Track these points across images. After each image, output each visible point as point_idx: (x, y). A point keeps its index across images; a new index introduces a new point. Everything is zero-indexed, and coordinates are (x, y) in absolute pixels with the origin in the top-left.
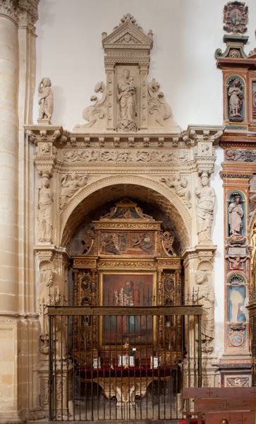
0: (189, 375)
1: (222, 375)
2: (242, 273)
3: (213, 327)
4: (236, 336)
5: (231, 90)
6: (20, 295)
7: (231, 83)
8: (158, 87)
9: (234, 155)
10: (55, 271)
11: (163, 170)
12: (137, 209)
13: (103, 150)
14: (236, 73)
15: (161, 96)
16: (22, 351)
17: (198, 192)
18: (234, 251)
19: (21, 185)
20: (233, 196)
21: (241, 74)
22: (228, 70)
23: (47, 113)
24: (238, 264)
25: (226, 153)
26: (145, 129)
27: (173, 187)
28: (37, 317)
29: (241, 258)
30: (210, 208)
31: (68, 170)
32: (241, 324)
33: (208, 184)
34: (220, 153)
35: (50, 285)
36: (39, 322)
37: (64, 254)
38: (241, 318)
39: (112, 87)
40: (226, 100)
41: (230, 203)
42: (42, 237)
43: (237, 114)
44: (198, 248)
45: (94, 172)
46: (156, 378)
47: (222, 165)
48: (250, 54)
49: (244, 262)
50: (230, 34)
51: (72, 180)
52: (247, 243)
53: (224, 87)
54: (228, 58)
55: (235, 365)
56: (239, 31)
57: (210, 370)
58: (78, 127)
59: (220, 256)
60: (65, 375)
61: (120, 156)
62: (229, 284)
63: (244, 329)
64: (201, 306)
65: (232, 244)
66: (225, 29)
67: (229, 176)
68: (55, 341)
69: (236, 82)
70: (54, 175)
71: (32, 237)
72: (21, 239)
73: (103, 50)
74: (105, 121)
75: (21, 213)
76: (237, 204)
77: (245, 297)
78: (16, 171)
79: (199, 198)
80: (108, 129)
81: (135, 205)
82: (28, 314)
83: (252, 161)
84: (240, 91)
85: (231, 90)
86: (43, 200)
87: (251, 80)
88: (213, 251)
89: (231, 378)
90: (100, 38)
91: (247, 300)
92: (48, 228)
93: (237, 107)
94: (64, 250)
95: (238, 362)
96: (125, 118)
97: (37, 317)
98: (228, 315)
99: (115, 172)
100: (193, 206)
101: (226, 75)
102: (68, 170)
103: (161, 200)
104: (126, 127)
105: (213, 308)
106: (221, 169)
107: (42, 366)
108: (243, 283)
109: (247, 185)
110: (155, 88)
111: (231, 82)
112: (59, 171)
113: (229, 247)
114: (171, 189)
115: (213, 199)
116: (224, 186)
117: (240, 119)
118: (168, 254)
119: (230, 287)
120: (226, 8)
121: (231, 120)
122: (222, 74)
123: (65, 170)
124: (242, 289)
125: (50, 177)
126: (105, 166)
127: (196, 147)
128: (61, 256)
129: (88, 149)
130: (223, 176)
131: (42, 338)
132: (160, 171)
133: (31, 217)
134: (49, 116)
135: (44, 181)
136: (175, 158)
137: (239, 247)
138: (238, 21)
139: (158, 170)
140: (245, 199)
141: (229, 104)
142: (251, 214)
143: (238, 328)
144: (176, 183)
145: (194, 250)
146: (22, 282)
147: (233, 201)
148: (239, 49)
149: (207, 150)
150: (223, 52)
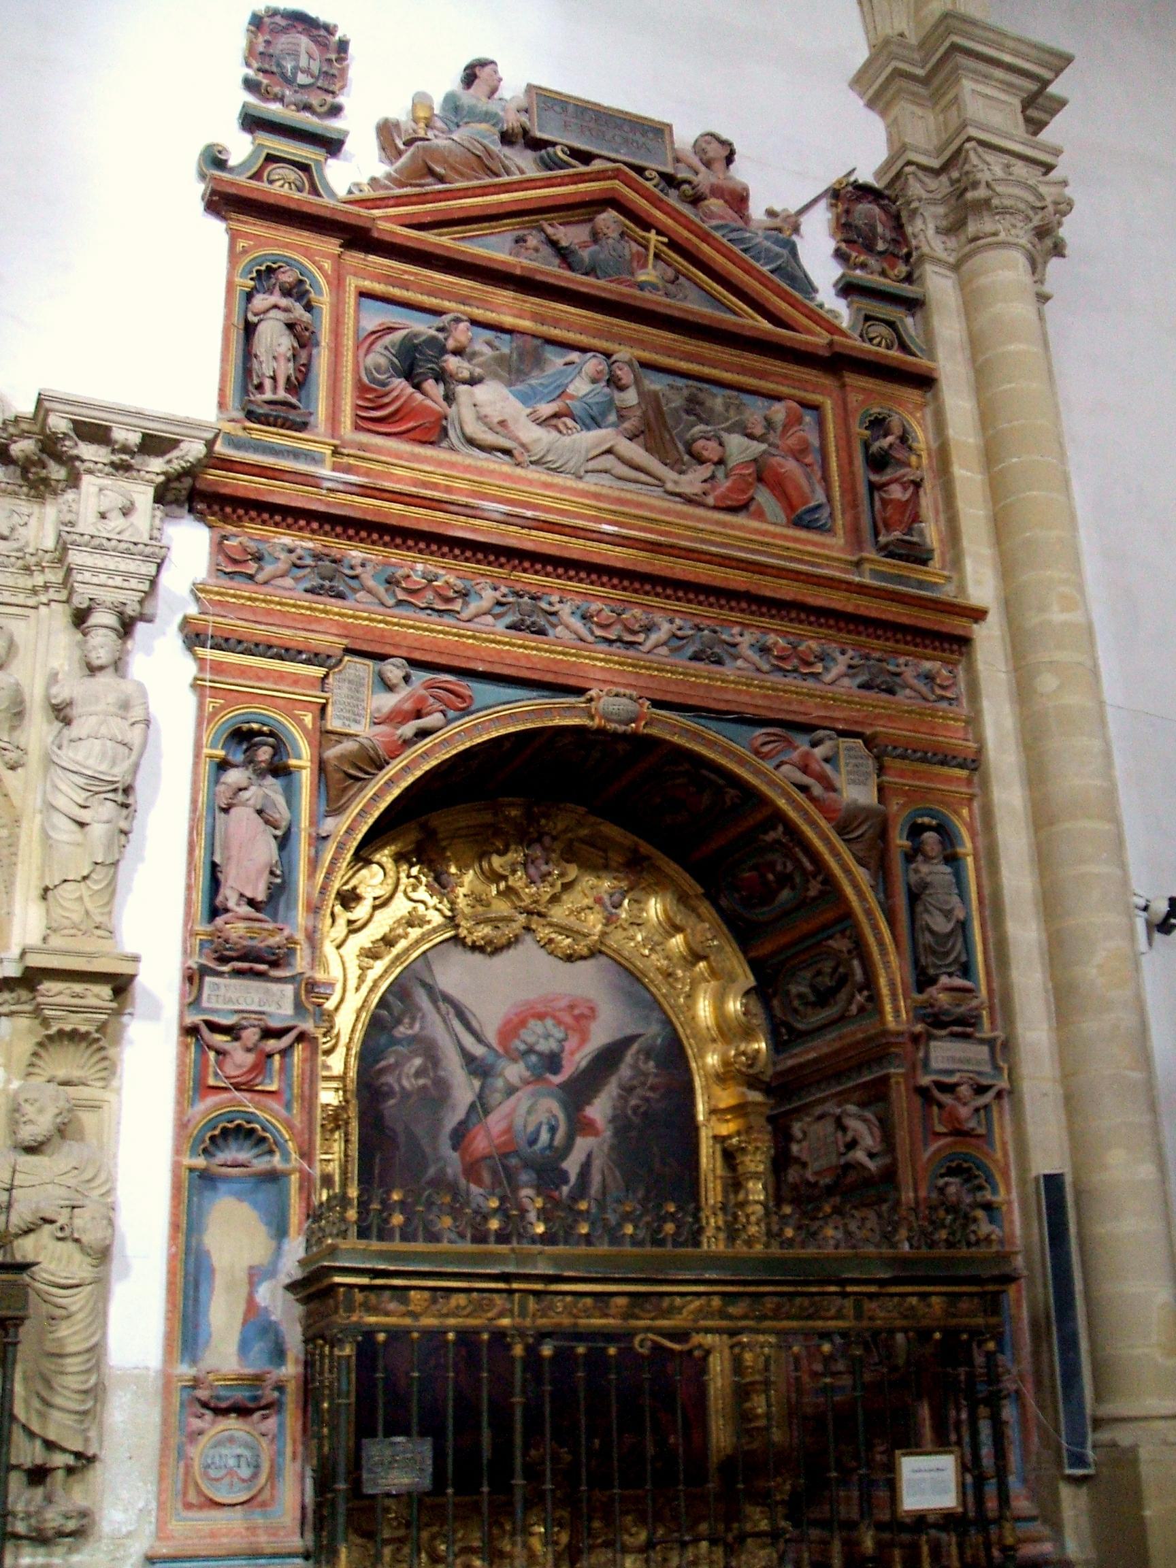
2: (267, 1114)
3: (96, 1393)
5: (260, 301)
9: (258, 558)
14: (287, 246)
17: (61, 693)
20: (242, 736)
24: (250, 1059)
25: (219, 546)
29: (269, 1033)
30: (119, 773)
32: (258, 1379)
33: (118, 665)
38: (259, 1347)
40: (237, 336)
41: (223, 765)
43: (282, 394)
44: (35, 961)
47: (198, 591)
48: (350, 192)
49: (285, 1053)
50: (274, 110)
52: (301, 963)
54: (254, 183)
56: (307, 107)
59: (155, 1013)
62: (200, 1162)
63: (274, 1406)
64: (24, 1267)
65: (223, 960)
66: (250, 85)
67: (224, 643)
69: (287, 277)
77: (280, 1231)
79: (67, 722)
83: (341, 596)
84: (299, 311)
87: (353, 284)
88: (121, 985)
91: (295, 1248)
93: (285, 369)
100: (34, 759)
101: (242, 243)
105: (101, 1285)
108: (276, 1161)
111: (265, 275)
113: (204, 971)
115: (135, 736)
117: (293, 415)
119: (205, 1180)
121: (251, 415)
122: (225, 239)
124: (267, 1193)
127: (70, 495)
130: (194, 637)
138: (307, 71)
140: (303, 759)
141: (248, 355)
142: (329, 825)
147: (239, 757)
148: (304, 168)
149: (126, 512)
150: (232, 162)
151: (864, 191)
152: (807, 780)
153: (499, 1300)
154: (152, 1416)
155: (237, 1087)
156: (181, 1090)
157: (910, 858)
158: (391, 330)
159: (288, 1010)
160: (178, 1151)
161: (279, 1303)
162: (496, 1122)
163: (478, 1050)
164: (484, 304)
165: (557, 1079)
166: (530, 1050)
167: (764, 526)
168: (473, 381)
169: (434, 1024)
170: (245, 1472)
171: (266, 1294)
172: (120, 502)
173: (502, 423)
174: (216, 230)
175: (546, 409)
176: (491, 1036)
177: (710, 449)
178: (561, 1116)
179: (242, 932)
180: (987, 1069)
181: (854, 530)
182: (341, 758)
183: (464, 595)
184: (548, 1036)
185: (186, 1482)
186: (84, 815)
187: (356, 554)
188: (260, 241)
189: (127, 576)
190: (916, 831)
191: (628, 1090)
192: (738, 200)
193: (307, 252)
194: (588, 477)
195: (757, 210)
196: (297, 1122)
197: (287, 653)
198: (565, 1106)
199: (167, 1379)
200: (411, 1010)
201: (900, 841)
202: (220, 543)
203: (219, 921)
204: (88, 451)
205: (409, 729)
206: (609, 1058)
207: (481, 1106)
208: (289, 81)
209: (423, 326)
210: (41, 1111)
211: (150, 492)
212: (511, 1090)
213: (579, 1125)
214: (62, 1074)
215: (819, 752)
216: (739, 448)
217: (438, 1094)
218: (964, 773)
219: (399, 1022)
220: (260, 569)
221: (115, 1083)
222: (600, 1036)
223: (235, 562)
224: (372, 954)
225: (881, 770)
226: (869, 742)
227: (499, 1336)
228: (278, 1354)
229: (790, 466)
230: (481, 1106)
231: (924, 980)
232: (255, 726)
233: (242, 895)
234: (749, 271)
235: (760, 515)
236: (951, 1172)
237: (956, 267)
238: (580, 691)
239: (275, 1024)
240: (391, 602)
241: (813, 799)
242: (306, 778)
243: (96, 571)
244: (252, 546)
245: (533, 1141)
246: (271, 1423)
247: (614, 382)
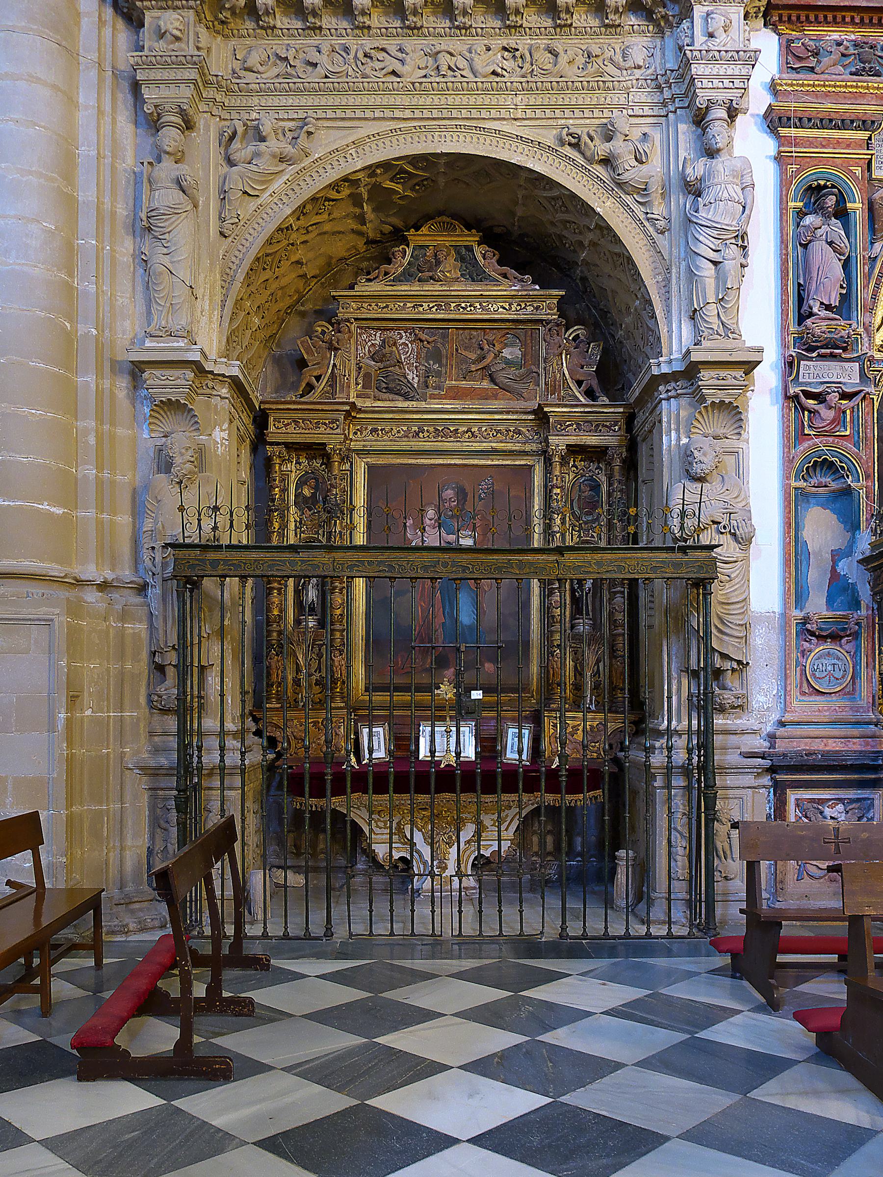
1: (779, 789)
12: (478, 251)
25: (787, 48)
29: (845, 396)
31: (249, 109)
37: (236, 385)
41: (801, 214)
45: (340, 114)
46: (550, 799)
55: (825, 754)
57: (739, 770)
62: (802, 484)
77: (853, 526)
81: (471, 239)
89: (812, 801)
99: (408, 114)
102: (249, 109)
103: (560, 216)
109: (863, 153)
118: (582, 399)
123: (238, 109)
126: (373, 91)
132: (563, 108)
137: (833, 357)
139: (553, 108)
145: (678, 367)
161: (855, 572)
171: (843, 567)
179: (824, 328)
185: (801, 679)
196: (863, 455)
197: (844, 124)
202: (788, 47)
203: (809, 322)
210: (705, 455)
220: (819, 62)
221: (744, 435)
223: (799, 59)
232: (822, 183)
233: (822, 303)
243: (710, 78)
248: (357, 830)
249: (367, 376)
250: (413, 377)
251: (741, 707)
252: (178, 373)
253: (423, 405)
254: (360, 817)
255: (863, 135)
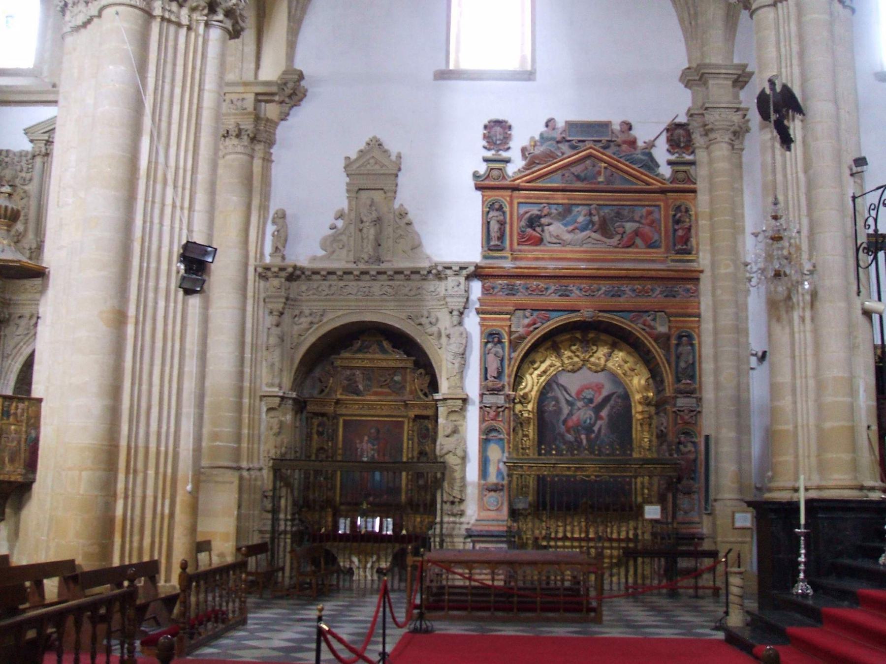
0: (435, 542)
2: (500, 426)
4: (492, 497)
5: (491, 214)
6: (242, 445)
7: (491, 207)
8: (406, 214)
9: (493, 288)
10: (283, 419)
11: (413, 306)
13: (342, 284)
15: (409, 224)
16: (242, 507)
17: (448, 332)
18: (490, 399)
19: (249, 325)
21: (504, 197)
22: (489, 193)
23: (280, 247)
24: (495, 413)
25: (483, 287)
26: (389, 261)
27: (420, 324)
28: (261, 469)
29: (498, 407)
34: (476, 287)
35: (278, 434)
36: (262, 476)
37: (294, 399)
38: (500, 477)
39: (353, 215)
41: (487, 343)
42: (270, 381)
49: (503, 411)
51: (306, 317)
53: (483, 211)
58: (314, 259)
59: (474, 403)
60: (289, 536)
61: (361, 289)
63: (502, 490)
68: (280, 497)
69: (497, 206)
70: (286, 311)
71: (258, 381)
72: (246, 384)
73: (345, 174)
74: (344, 252)
75: (248, 355)
76: (495, 345)
77: (503, 452)
78: (244, 310)
80: (347, 262)
82: (251, 466)
83: (514, 295)
85: (490, 216)
86: (273, 340)
87: (516, 201)
90: (342, 164)
92: (276, 369)
94: (294, 395)
95: (492, 528)
96: (365, 250)
97: (261, 469)
98: (484, 472)
100: (444, 347)
101: (485, 198)
104: (367, 262)
106: (478, 306)
107: (264, 525)
108: (501, 436)
110: (403, 214)
111: (491, 207)
112: (291, 307)
114: (419, 327)
116: (482, 326)
120: (486, 127)
121: (490, 250)
122: (481, 197)
125: (282, 314)
128: (290, 402)
129: (325, 282)
130: (478, 313)
131: (266, 494)
133: (259, 359)
134: (282, 249)
135: (274, 319)
136: (424, 292)
137: (497, 394)
138: (499, 140)
140: (506, 340)
142: (514, 355)
143: (495, 489)
144: (424, 321)
146: (245, 431)
151: (680, 126)
152: (644, 327)
153: (544, 468)
154: (476, 491)
155: (492, 420)
156: (480, 421)
157: (678, 345)
158: (527, 213)
159: (503, 402)
160: (480, 435)
162: (575, 418)
163: (570, 399)
164: (553, 198)
165: (592, 405)
166: (585, 398)
167: (554, 320)
168: (549, 225)
169: (558, 393)
170: (495, 503)
172: (457, 284)
173: (558, 236)
174: (479, 194)
175: (570, 228)
176: (573, 394)
177: (620, 230)
178: (593, 415)
180: (695, 405)
181: (667, 247)
182: (515, 338)
183: (547, 289)
184: (590, 394)
186: (454, 361)
187: (518, 282)
188: (490, 197)
189: (459, 302)
190: (680, 337)
191: (612, 408)
192: (633, 143)
193: (503, 196)
194: (585, 245)
195: (640, 143)
198: (594, 414)
199: (479, 484)
200: (552, 389)
201: (674, 342)
204: (448, 272)
205: (531, 329)
206: (607, 399)
207: (570, 414)
208: (495, 144)
209: (535, 210)
211: (464, 278)
212: (579, 409)
213: (598, 417)
214: (453, 419)
215: (649, 318)
216: (630, 227)
217: (559, 411)
218: (697, 319)
219: (548, 393)
222: (605, 393)
223: (487, 290)
224: (540, 376)
225: (670, 321)
226: (666, 313)
227: (544, 476)
228: (503, 479)
229: (647, 229)
230: (570, 414)
231: (679, 380)
234: (634, 169)
235: (637, 247)
236: (684, 433)
237: (707, 148)
238: (579, 311)
239: (499, 405)
240: (527, 294)
241: (646, 332)
242: (507, 344)
243: (452, 302)
244: (491, 285)
245: (585, 422)
246: (501, 493)
247: (591, 214)
248: (333, 555)
249: (343, 387)
250: (361, 387)
251: (462, 514)
252: (275, 399)
253: (363, 398)
254: (334, 551)
255: (508, 316)
